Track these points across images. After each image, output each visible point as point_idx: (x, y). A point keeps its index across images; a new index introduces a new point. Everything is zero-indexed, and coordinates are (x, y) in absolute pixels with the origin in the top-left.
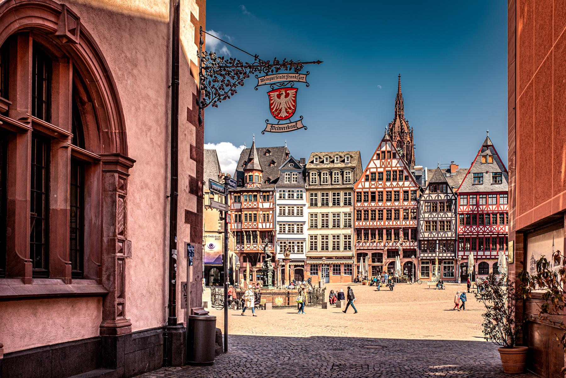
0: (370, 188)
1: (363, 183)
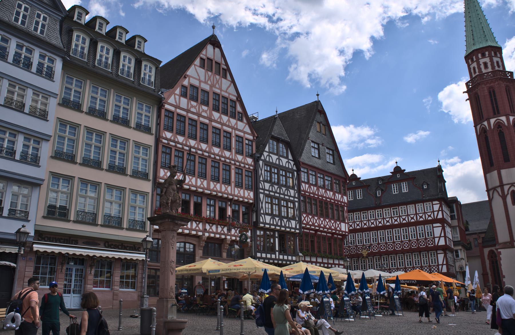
0: (188, 111)
1: (177, 97)
